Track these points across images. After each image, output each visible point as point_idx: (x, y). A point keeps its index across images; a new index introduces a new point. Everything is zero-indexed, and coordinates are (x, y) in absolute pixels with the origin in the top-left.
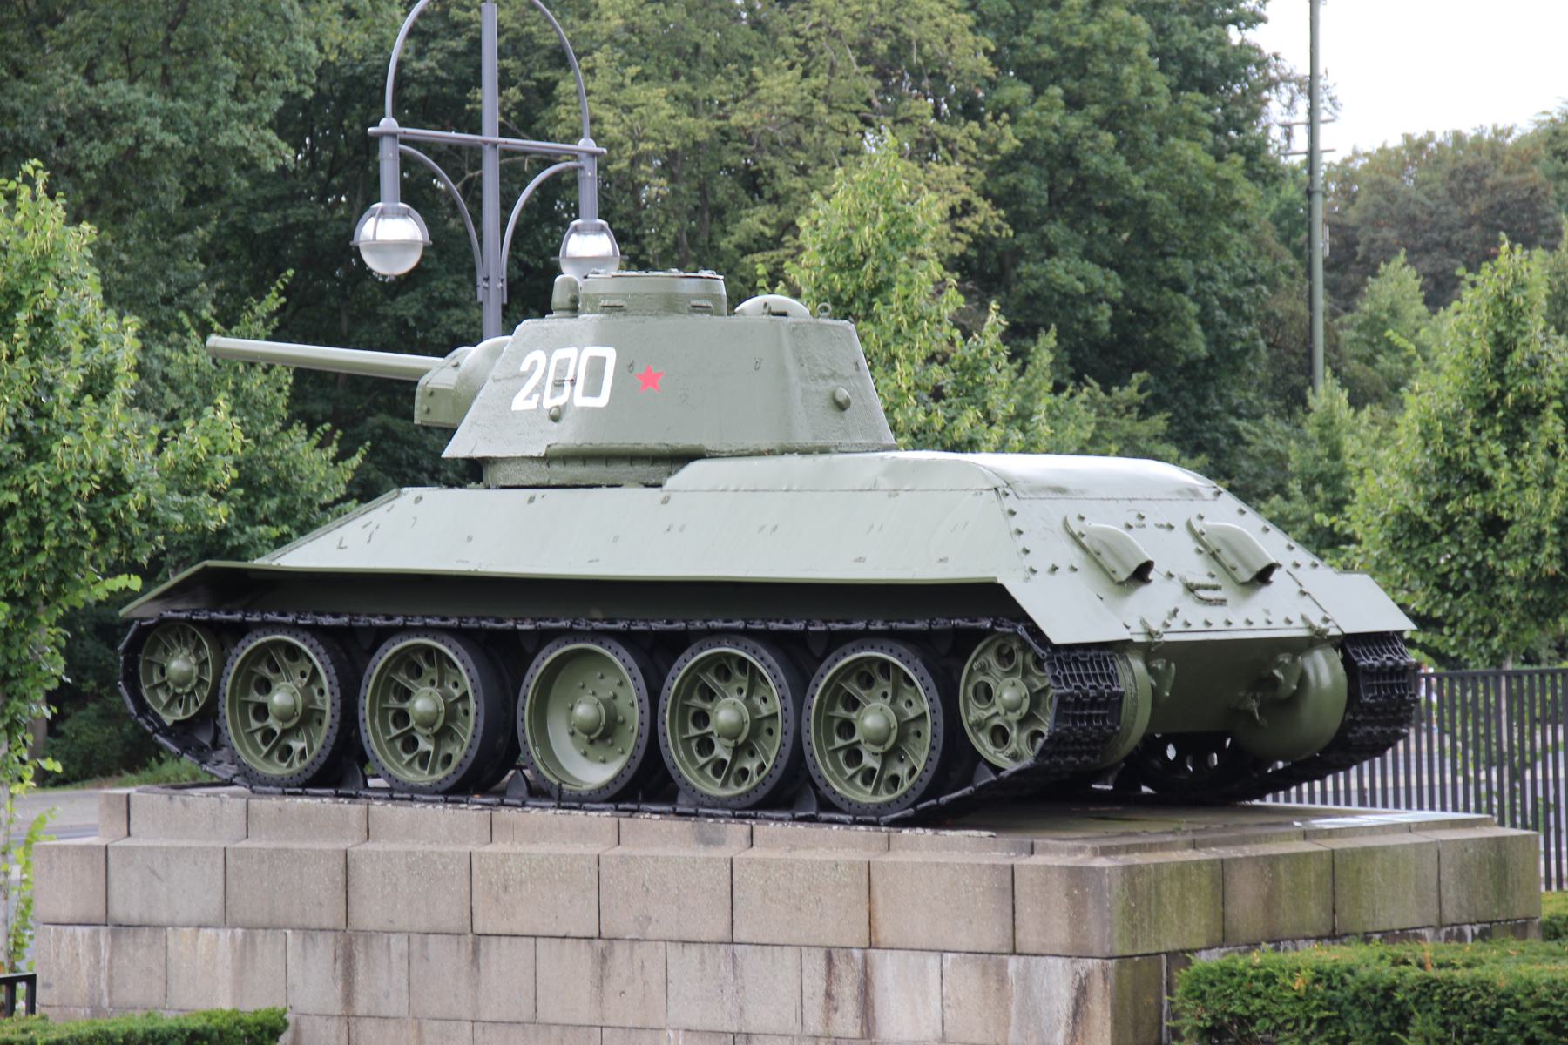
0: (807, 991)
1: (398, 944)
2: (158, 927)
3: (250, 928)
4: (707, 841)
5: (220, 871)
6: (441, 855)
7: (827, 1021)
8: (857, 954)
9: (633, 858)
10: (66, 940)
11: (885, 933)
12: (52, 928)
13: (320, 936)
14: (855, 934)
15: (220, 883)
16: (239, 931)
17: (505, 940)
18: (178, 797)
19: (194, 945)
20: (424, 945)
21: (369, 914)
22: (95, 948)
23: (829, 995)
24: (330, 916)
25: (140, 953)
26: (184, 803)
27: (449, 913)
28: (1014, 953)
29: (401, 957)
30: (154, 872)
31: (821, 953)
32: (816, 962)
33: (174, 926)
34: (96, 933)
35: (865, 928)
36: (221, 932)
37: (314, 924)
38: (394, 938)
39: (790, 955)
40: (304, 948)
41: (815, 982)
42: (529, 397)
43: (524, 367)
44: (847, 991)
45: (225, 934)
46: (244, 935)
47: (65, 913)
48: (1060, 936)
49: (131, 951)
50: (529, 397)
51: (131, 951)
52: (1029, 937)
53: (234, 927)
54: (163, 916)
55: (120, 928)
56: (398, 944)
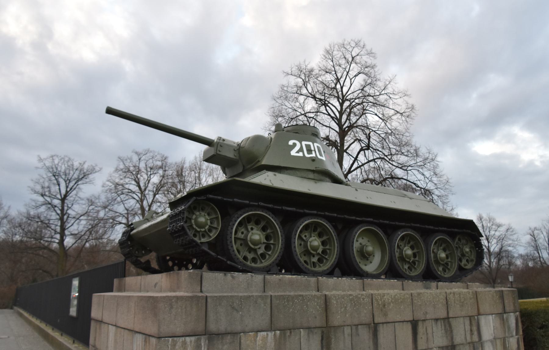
0: (467, 329)
1: (347, 330)
2: (234, 334)
3: (282, 330)
4: (427, 288)
5: (269, 306)
6: (362, 295)
7: (471, 338)
8: (476, 317)
9: (421, 293)
10: (179, 344)
11: (482, 311)
12: (170, 339)
13: (316, 330)
14: (475, 312)
15: (269, 311)
16: (278, 332)
17: (385, 325)
18: (229, 275)
19: (255, 341)
20: (357, 329)
21: (336, 320)
22: (198, 347)
23: (471, 330)
24: (319, 322)
25: (226, 347)
26: (233, 277)
27: (365, 317)
28: (505, 313)
29: (348, 335)
30: (233, 308)
31: (468, 318)
32: (467, 322)
33: (244, 332)
34: (199, 340)
35: (476, 310)
36: (269, 333)
37: (313, 325)
38: (346, 328)
39: (462, 319)
40: (308, 336)
41: (468, 327)
42: (298, 152)
43: (291, 143)
44: (475, 328)
45: (271, 335)
46: (280, 334)
47: (179, 330)
48: (512, 308)
49: (220, 347)
50: (298, 152)
51: (220, 347)
52: (507, 309)
53: (275, 331)
54: (238, 328)
55: (212, 336)
56: (347, 330)
